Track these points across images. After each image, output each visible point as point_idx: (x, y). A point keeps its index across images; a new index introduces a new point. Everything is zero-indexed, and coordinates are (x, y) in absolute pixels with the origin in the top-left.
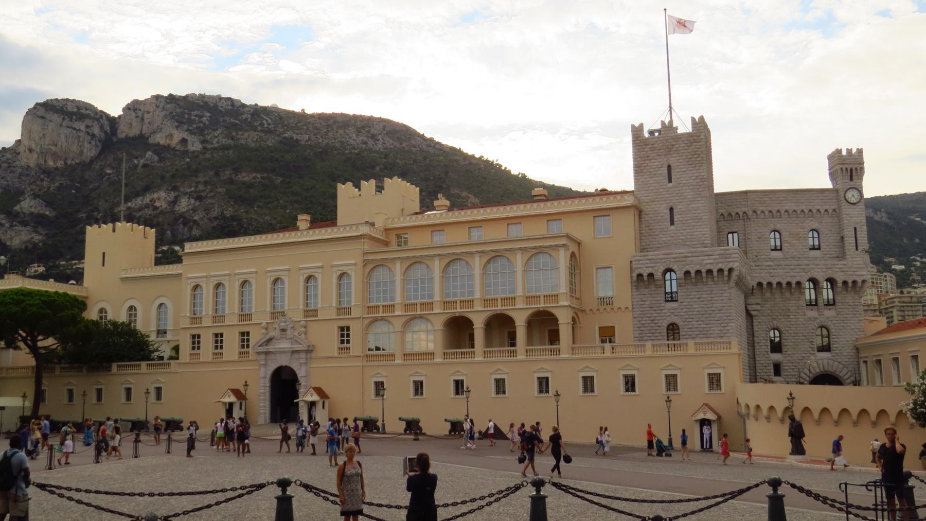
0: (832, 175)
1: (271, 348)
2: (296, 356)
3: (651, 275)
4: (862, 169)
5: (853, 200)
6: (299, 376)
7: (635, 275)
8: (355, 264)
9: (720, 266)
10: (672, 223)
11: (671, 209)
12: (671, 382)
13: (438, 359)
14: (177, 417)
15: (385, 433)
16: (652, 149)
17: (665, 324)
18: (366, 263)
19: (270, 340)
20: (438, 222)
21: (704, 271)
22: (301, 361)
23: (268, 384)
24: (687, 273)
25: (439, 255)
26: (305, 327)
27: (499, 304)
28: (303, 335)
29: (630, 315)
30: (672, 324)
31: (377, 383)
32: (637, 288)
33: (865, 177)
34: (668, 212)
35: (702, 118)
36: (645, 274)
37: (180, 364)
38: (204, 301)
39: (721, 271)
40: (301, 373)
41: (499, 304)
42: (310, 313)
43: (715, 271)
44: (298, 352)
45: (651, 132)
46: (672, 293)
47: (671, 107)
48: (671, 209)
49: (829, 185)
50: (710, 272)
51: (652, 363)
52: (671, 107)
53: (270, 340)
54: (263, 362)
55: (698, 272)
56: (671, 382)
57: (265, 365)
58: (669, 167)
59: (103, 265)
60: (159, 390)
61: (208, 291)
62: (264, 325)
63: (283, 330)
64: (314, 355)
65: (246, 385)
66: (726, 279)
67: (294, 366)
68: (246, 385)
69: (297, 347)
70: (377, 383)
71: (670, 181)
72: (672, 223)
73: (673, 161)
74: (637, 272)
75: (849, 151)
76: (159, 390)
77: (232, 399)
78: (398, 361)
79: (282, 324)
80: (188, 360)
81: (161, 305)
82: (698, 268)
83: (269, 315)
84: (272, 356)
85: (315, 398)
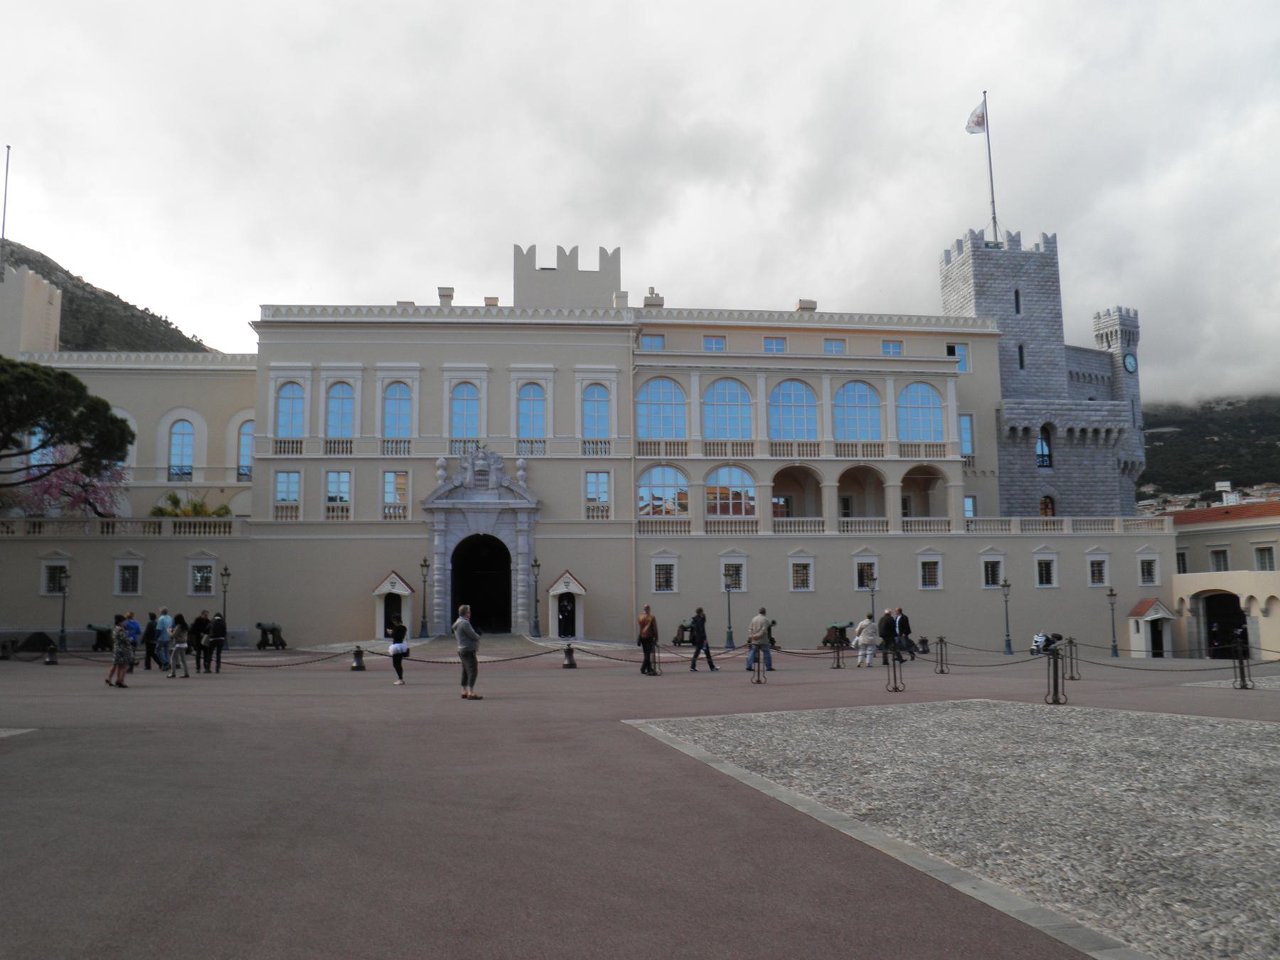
0: (1100, 337)
2: (508, 518)
3: (1026, 430)
4: (1138, 333)
5: (1130, 368)
6: (512, 553)
7: (1007, 428)
8: (619, 372)
9: (1109, 425)
10: (1022, 367)
11: (1021, 348)
12: (1097, 570)
13: (765, 532)
15: (733, 648)
16: (998, 266)
17: (1039, 497)
18: (638, 370)
20: (719, 322)
21: (1090, 430)
22: (519, 527)
23: (449, 566)
24: (1071, 431)
25: (767, 370)
26: (525, 470)
27: (860, 453)
29: (996, 481)
30: (1047, 497)
32: (1002, 445)
33: (1139, 343)
34: (1017, 350)
35: (1054, 236)
36: (1020, 428)
37: (251, 524)
39: (1108, 431)
41: (860, 453)
43: (1103, 430)
44: (514, 511)
45: (987, 245)
46: (1043, 456)
47: (994, 218)
48: (1021, 348)
49: (1093, 344)
50: (1096, 431)
51: (1021, 544)
52: (994, 218)
54: (442, 527)
55: (1083, 431)
56: (1097, 570)
58: (1017, 293)
63: (483, 473)
64: (538, 518)
66: (1112, 442)
67: (504, 536)
68: (425, 565)
69: (512, 502)
71: (1018, 311)
72: (1022, 367)
73: (1022, 285)
74: (1012, 424)
75: (1128, 311)
80: (271, 519)
82: (1083, 425)
84: (459, 517)
85: (574, 588)
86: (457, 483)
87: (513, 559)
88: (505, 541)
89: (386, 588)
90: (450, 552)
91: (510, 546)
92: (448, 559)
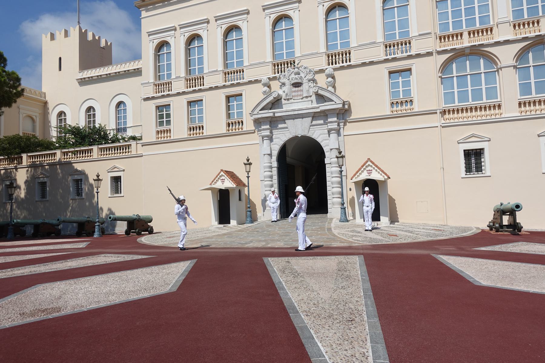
1: (278, 113)
6: (326, 149)
14: (143, 213)
19: (276, 103)
23: (275, 164)
28: (330, 89)
31: (468, 154)
38: (173, 62)
40: (329, 144)
42: (339, 58)
53: (276, 103)
57: (271, 139)
59: (60, 69)
60: (117, 180)
61: (178, 45)
62: (265, 79)
63: (297, 85)
65: (248, 163)
67: (319, 134)
68: (248, 163)
70: (468, 154)
76: (117, 180)
77: (228, 184)
78: (510, 110)
79: (293, 76)
81: (120, 104)
83: (270, 67)
85: (376, 176)
86: (274, 95)
87: (327, 154)
88: (319, 140)
89: (220, 185)
90: (275, 153)
91: (322, 144)
92: (274, 158)
